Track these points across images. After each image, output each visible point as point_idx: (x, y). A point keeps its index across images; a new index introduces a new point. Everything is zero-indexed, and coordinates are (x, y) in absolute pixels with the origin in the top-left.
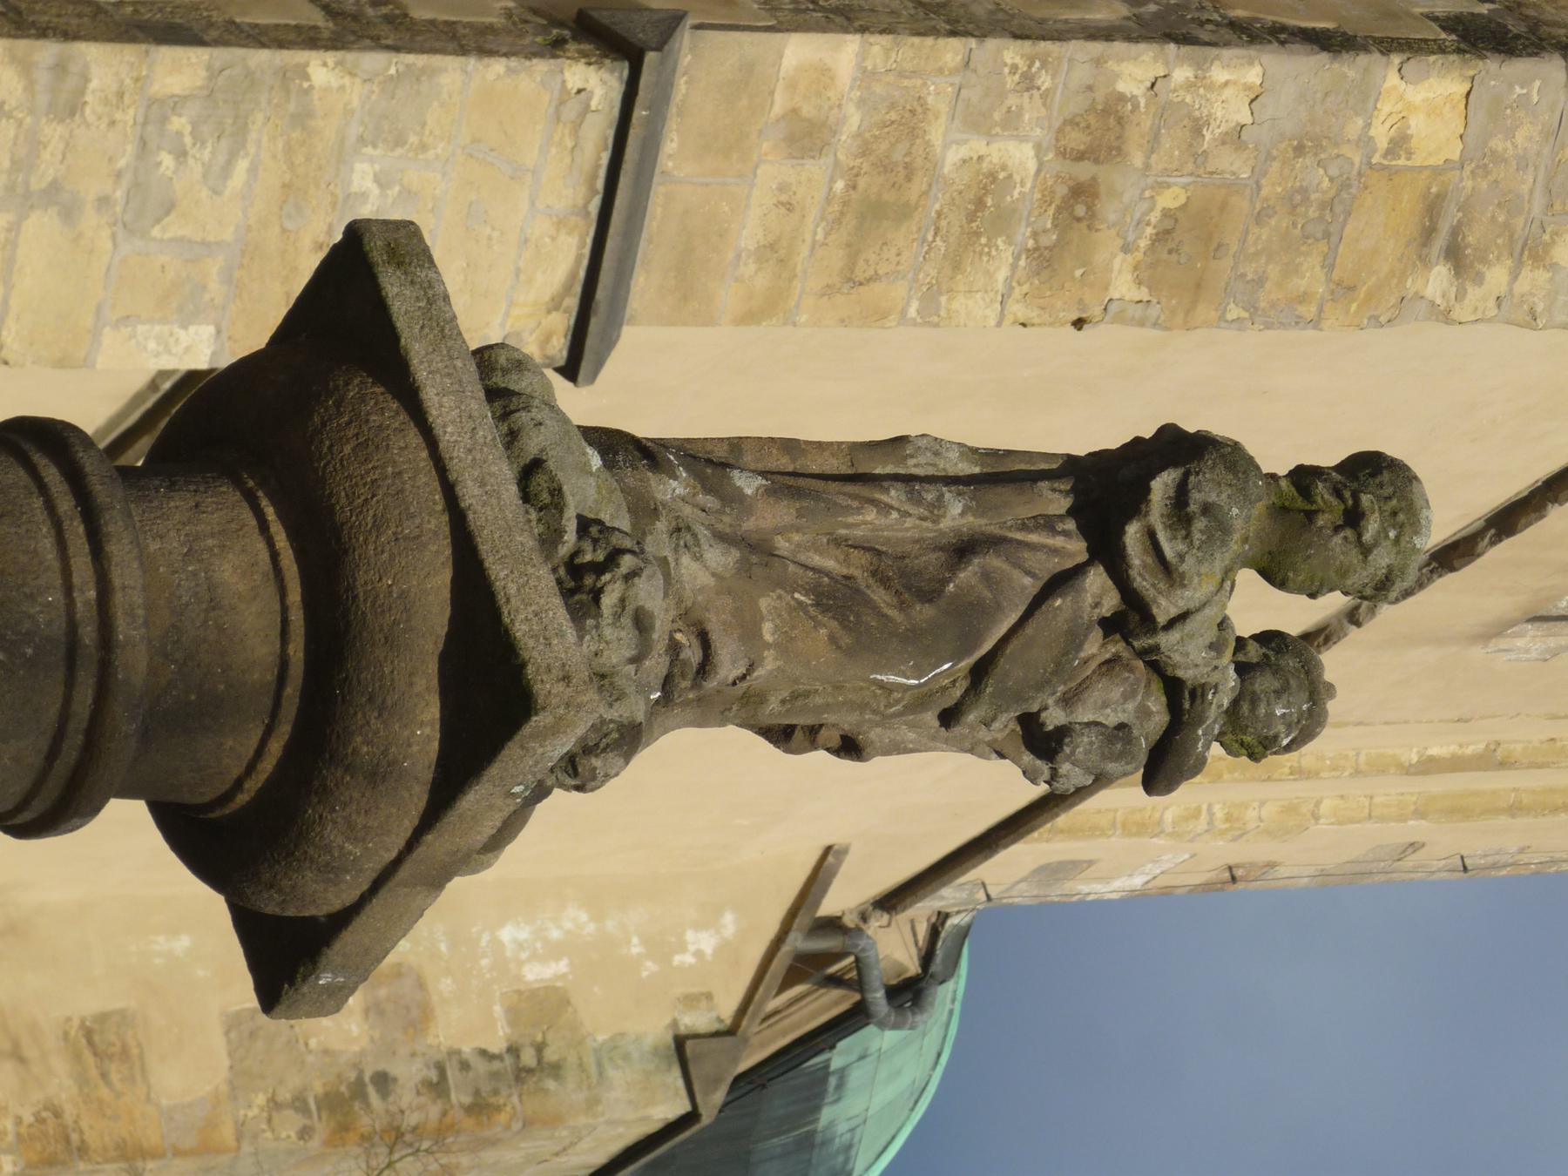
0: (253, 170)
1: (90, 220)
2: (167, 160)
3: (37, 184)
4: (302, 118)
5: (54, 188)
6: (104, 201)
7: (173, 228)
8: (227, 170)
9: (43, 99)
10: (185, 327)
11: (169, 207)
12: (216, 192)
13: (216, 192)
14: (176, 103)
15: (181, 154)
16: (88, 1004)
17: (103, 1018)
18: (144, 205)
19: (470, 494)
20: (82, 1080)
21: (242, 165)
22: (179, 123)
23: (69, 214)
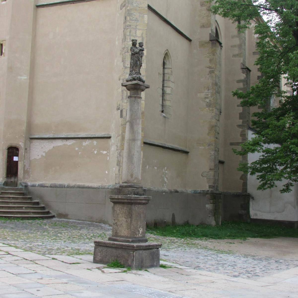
0: (134, 13)
1: (138, 24)
2: (134, 19)
3: (135, 27)
4: (131, 9)
5: (136, 26)
6: (136, 23)
7: (138, 18)
8: (134, 15)
9: (130, 27)
10: (144, 17)
11: (137, 18)
12: (136, 15)
13: (136, 15)
14: (130, 18)
15: (133, 18)
16: (199, 5)
17: (200, 4)
18: (137, 20)
19: (130, 84)
20: (205, 6)
21: (134, 14)
22: (131, 18)
23: (137, 25)
